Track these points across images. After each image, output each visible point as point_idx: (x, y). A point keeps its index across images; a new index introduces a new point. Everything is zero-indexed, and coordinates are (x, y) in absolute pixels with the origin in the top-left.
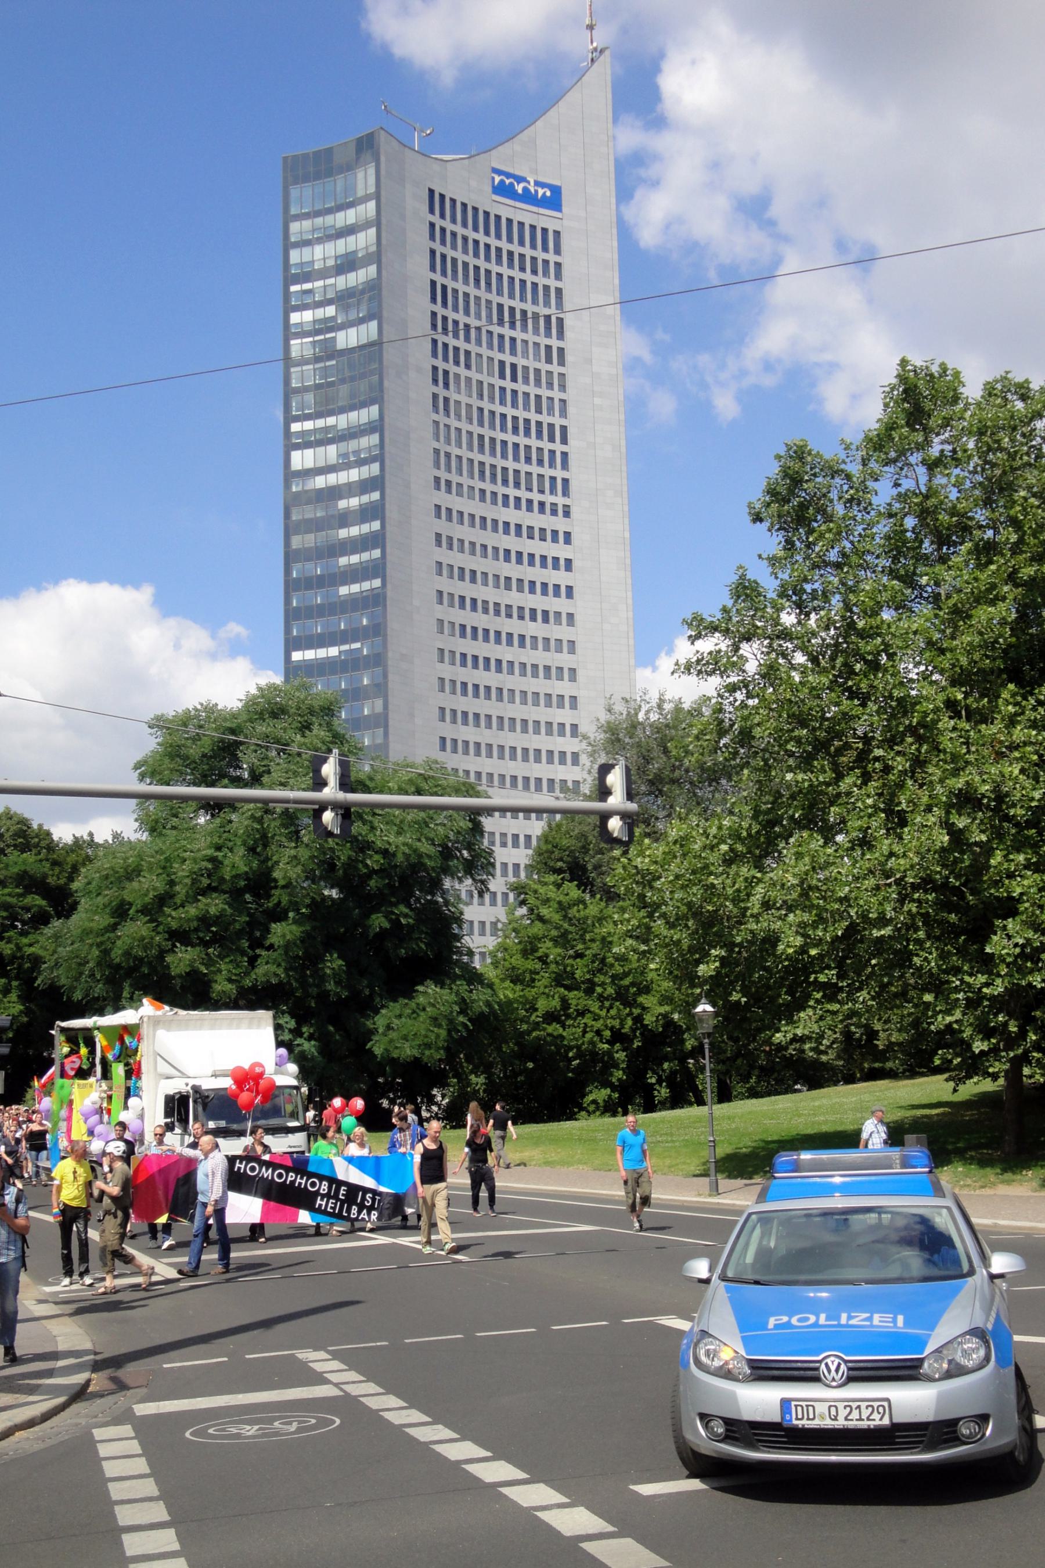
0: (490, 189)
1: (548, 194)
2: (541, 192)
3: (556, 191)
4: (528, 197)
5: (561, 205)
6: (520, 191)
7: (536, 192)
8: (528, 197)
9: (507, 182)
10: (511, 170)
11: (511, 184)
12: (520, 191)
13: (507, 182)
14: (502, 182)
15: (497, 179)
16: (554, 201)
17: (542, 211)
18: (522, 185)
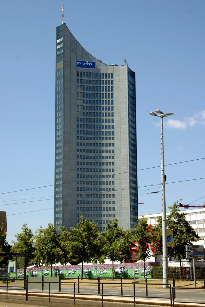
0: (76, 66)
1: (92, 64)
2: (90, 64)
3: (94, 63)
4: (86, 66)
5: (95, 67)
6: (84, 65)
7: (88, 64)
8: (86, 66)
9: (81, 63)
10: (82, 61)
11: (82, 64)
12: (84, 65)
13: (81, 63)
14: (79, 64)
15: (78, 63)
16: (93, 65)
17: (90, 69)
18: (84, 64)
